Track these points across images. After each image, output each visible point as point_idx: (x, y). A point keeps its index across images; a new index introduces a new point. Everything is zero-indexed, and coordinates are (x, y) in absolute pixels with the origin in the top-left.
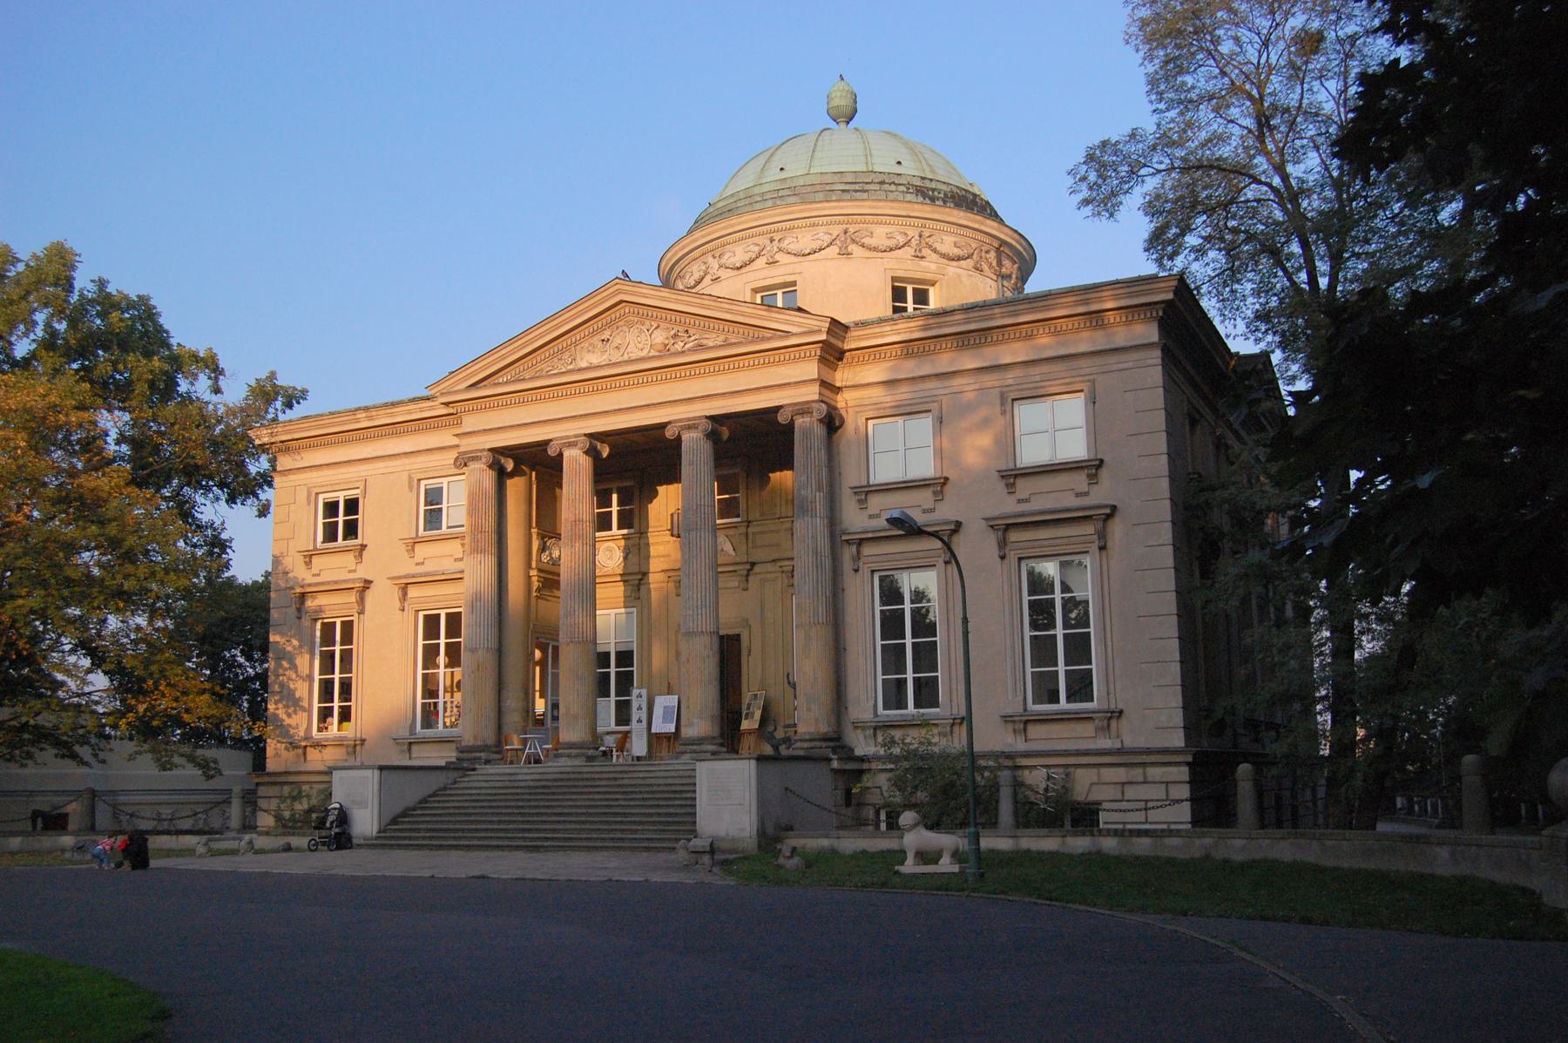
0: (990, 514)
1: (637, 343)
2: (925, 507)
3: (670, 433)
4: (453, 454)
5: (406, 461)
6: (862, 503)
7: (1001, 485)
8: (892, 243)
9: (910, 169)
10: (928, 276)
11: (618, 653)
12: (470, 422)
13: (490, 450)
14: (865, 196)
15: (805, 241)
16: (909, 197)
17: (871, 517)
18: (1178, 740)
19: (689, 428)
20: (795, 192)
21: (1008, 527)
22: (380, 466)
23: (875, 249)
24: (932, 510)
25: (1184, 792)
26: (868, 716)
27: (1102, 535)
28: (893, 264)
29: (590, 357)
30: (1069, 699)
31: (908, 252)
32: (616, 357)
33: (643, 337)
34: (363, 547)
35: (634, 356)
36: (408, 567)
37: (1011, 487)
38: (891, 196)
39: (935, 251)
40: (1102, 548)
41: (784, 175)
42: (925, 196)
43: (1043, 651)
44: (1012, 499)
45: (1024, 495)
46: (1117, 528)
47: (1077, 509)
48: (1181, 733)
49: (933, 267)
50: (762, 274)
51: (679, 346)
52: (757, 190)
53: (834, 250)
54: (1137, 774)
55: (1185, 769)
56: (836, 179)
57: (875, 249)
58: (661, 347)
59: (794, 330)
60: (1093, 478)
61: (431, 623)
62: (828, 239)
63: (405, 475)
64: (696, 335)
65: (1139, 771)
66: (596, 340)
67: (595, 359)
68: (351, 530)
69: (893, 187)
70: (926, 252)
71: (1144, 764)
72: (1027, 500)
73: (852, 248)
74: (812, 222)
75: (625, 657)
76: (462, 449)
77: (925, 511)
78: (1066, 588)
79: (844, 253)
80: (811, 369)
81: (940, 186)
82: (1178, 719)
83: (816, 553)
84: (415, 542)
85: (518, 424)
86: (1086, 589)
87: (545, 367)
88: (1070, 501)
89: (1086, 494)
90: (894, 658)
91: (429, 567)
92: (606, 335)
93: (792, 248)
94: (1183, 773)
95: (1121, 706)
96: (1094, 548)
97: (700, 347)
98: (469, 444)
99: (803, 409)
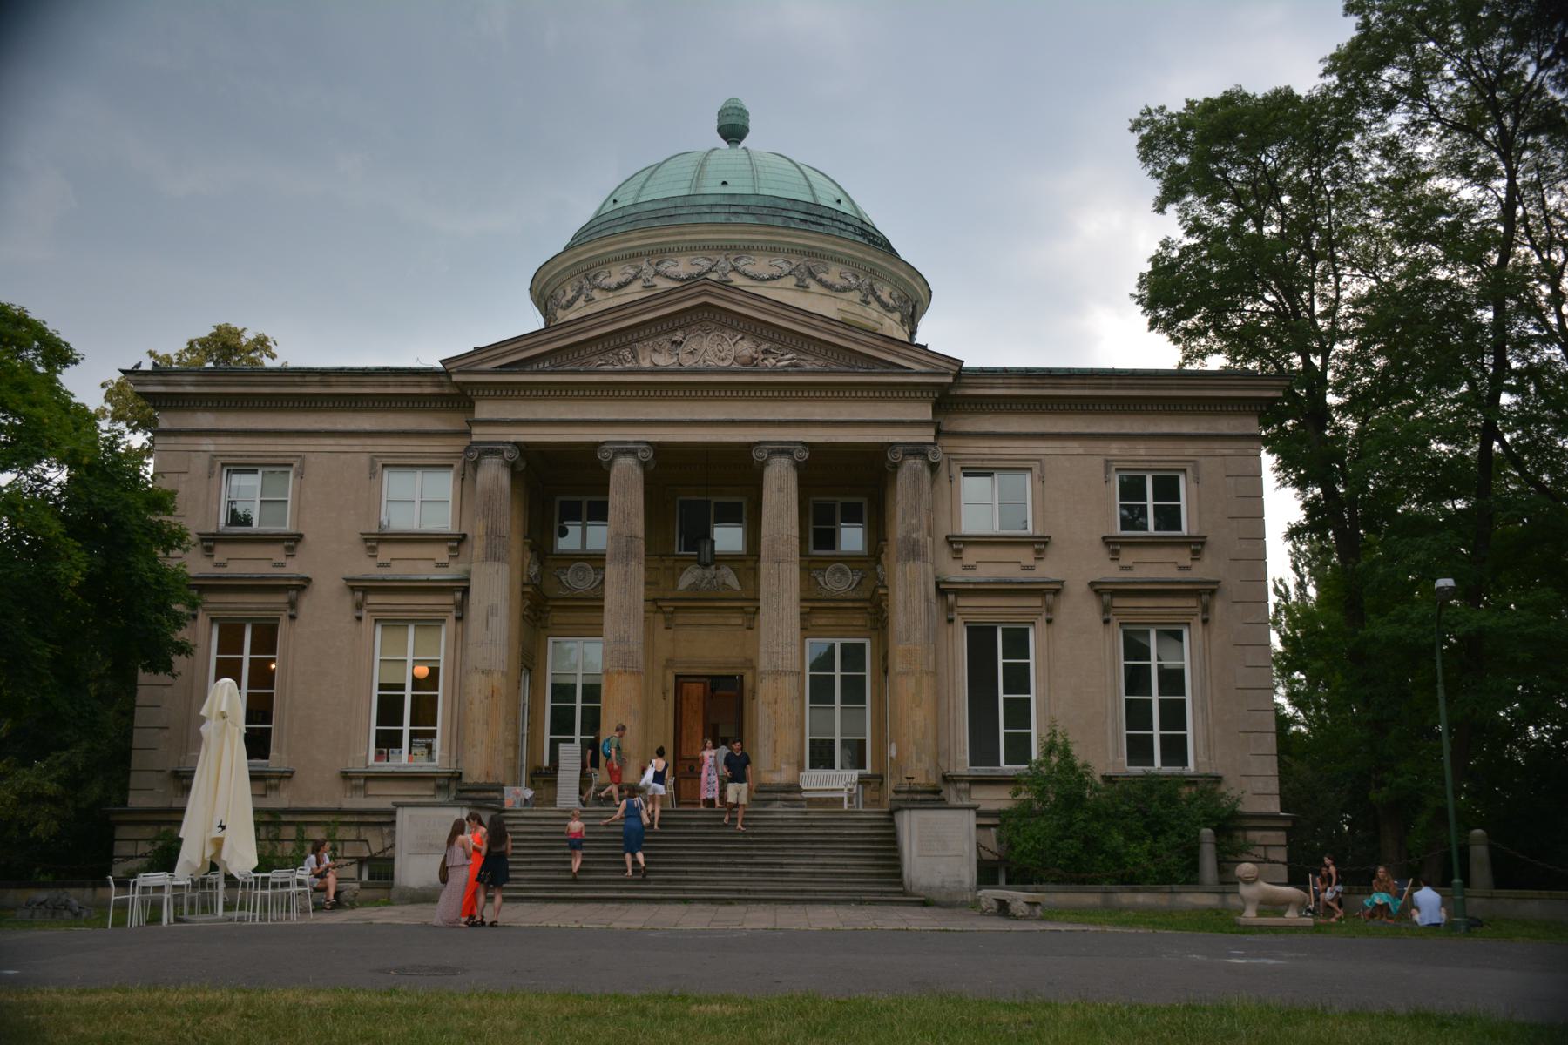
0: (1097, 578)
1: (715, 352)
2: (1025, 563)
4: (465, 442)
5: (369, 441)
6: (957, 554)
7: (1103, 553)
8: (845, 283)
11: (584, 686)
12: (483, 410)
13: (515, 443)
14: (821, 229)
16: (859, 239)
17: (966, 568)
18: (1273, 806)
19: (782, 452)
20: (749, 209)
21: (1116, 593)
22: (329, 444)
23: (830, 287)
24: (1031, 568)
27: (1206, 609)
28: (843, 305)
29: (656, 358)
30: (1163, 764)
31: (855, 296)
32: (689, 362)
33: (725, 345)
36: (366, 568)
38: (845, 234)
39: (878, 299)
40: (1205, 622)
43: (1137, 715)
44: (1115, 566)
45: (1128, 563)
46: (1218, 606)
47: (1179, 582)
48: (1277, 800)
49: (875, 315)
51: (770, 362)
52: (699, 200)
53: (791, 281)
55: (1282, 834)
56: (789, 205)
57: (830, 287)
58: (747, 360)
59: (917, 367)
60: (1196, 555)
62: (786, 268)
63: (364, 459)
64: (790, 357)
66: (664, 341)
67: (663, 360)
70: (870, 298)
73: (809, 281)
74: (773, 250)
76: (475, 438)
77: (1025, 568)
78: (1159, 659)
79: (802, 287)
80: (925, 412)
82: (1274, 786)
83: (927, 600)
86: (1186, 659)
87: (597, 361)
88: (1172, 573)
89: (1188, 568)
91: (399, 571)
92: (678, 336)
93: (748, 269)
94: (1279, 837)
95: (1220, 772)
97: (796, 368)
98: (480, 434)
99: (917, 450)
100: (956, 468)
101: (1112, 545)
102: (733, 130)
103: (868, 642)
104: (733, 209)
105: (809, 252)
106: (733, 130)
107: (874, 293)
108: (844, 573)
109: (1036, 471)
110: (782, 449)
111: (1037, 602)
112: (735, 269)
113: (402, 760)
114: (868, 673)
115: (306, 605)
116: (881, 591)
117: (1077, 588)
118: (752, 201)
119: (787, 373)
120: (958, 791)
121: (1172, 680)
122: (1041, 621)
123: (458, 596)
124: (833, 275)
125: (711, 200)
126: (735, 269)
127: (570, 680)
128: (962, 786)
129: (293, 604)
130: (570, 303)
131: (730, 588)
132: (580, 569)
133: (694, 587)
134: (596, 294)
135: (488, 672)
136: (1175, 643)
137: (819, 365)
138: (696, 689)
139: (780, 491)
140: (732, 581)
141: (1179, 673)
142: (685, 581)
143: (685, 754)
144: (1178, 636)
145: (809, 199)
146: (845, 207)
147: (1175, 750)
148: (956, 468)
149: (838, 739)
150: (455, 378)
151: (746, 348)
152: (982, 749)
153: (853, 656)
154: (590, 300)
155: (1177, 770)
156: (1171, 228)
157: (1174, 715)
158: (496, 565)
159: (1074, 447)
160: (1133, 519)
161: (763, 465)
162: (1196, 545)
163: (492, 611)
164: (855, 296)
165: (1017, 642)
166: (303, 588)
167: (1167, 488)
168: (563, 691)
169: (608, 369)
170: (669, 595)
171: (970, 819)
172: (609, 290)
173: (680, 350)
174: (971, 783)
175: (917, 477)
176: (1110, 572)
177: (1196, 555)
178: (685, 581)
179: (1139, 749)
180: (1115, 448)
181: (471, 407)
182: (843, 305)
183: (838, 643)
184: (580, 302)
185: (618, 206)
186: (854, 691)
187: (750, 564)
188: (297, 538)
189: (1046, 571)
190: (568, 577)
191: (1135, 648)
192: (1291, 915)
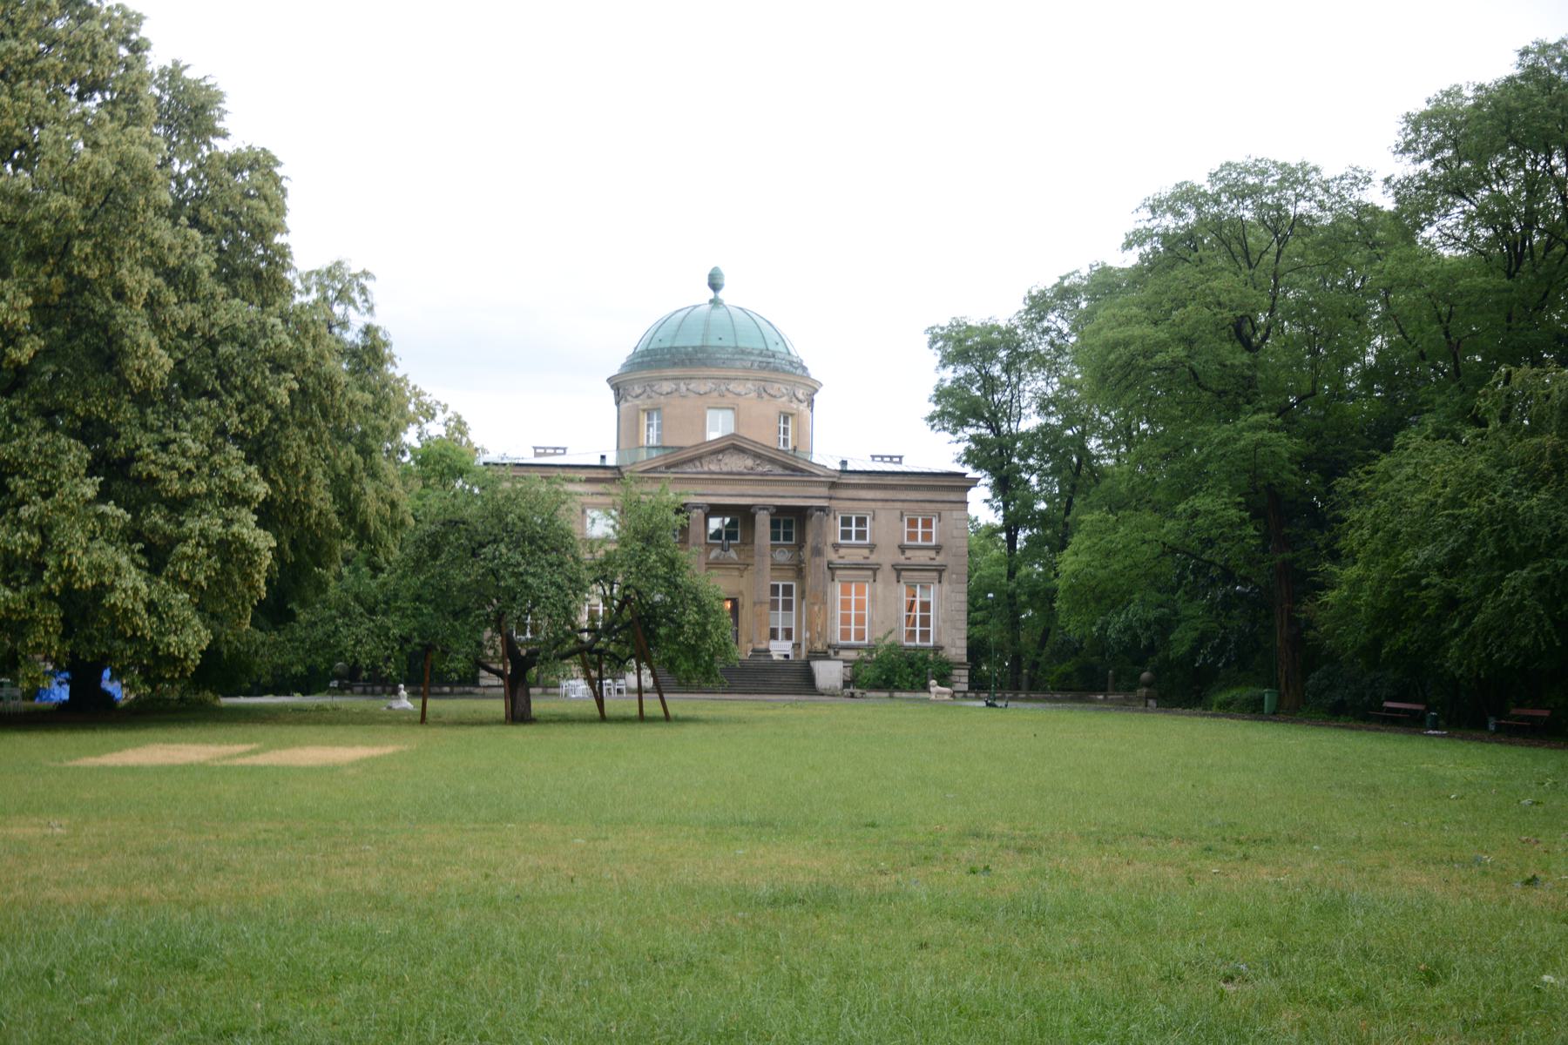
18: (965, 659)
32: (725, 469)
37: (903, 552)
41: (719, 343)
43: (910, 621)
46: (945, 575)
51: (760, 469)
64: (767, 467)
67: (714, 467)
90: (846, 620)
99: (821, 509)
102: (715, 283)
105: (765, 380)
106: (715, 283)
110: (764, 508)
117: (887, 567)
121: (925, 606)
139: (763, 521)
142: (713, 555)
145: (762, 346)
146: (781, 348)
147: (925, 635)
151: (749, 462)
153: (788, 590)
156: (949, 375)
157: (925, 621)
171: (841, 664)
175: (821, 520)
176: (901, 559)
178: (713, 555)
179: (911, 634)
186: (788, 606)
189: (874, 559)
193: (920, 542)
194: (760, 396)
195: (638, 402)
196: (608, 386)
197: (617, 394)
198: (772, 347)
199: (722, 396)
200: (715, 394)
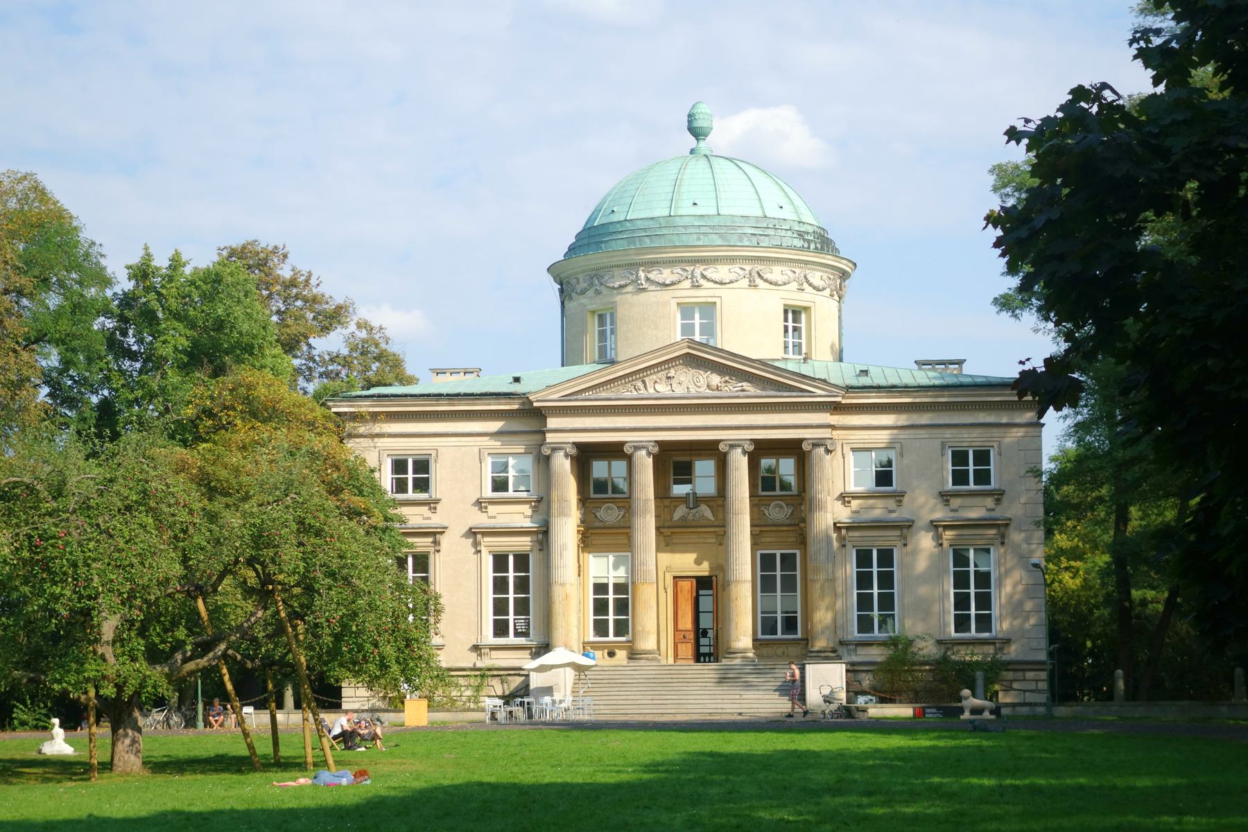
3: (722, 447)
8: (785, 278)
9: (788, 214)
10: (805, 304)
12: (552, 423)
15: (721, 272)
18: (1043, 656)
23: (776, 284)
25: (1043, 685)
26: (850, 638)
27: (1003, 536)
28: (785, 295)
30: (977, 631)
32: (679, 391)
34: (437, 501)
35: (693, 390)
36: (480, 520)
42: (805, 240)
50: (685, 292)
52: (679, 221)
54: (1019, 675)
57: (776, 284)
59: (819, 392)
60: (998, 501)
61: (500, 562)
63: (476, 450)
65: (1021, 673)
66: (662, 375)
67: (663, 388)
68: (422, 485)
69: (783, 233)
70: (806, 286)
71: (1024, 670)
72: (955, 510)
73: (758, 281)
74: (732, 260)
75: (620, 588)
78: (976, 566)
79: (752, 285)
81: (810, 229)
84: (480, 504)
85: (597, 429)
92: (672, 373)
96: (998, 542)
100: (847, 449)
101: (945, 497)
103: (798, 552)
104: (703, 230)
107: (808, 281)
108: (781, 507)
109: (898, 449)
111: (898, 533)
112: (704, 277)
113: (511, 639)
114: (798, 573)
115: (444, 540)
116: (802, 525)
118: (716, 221)
119: (738, 397)
120: (849, 651)
121: (983, 579)
122: (899, 544)
123: (540, 536)
124: (776, 273)
125: (686, 221)
126: (704, 277)
127: (604, 581)
128: (852, 647)
129: (436, 543)
130: (583, 292)
131: (707, 519)
132: (609, 508)
133: (683, 518)
134: (603, 289)
135: (563, 585)
136: (984, 555)
137: (759, 392)
138: (687, 586)
140: (708, 513)
141: (988, 574)
143: (680, 627)
144: (988, 551)
148: (847, 449)
149: (779, 616)
150: (535, 404)
151: (716, 379)
152: (865, 624)
153: (788, 561)
154: (598, 293)
155: (986, 635)
158: (564, 519)
159: (923, 433)
160: (960, 478)
161: (725, 455)
162: (998, 495)
163: (564, 547)
164: (794, 286)
165: (886, 557)
166: (442, 533)
167: (982, 457)
168: (600, 588)
169: (627, 394)
170: (667, 524)
172: (613, 288)
173: (674, 382)
174: (857, 645)
177: (998, 501)
179: (962, 623)
180: (948, 433)
181: (545, 418)
182: (785, 295)
183: (778, 553)
184: (591, 293)
185: (615, 218)
187: (720, 502)
188: (437, 501)
190: (601, 514)
191: (960, 559)
192: (986, 715)
193: (972, 486)
194: (752, 285)
195: (584, 300)
196: (549, 279)
197: (562, 291)
198: (772, 212)
199: (696, 286)
200: (687, 284)
